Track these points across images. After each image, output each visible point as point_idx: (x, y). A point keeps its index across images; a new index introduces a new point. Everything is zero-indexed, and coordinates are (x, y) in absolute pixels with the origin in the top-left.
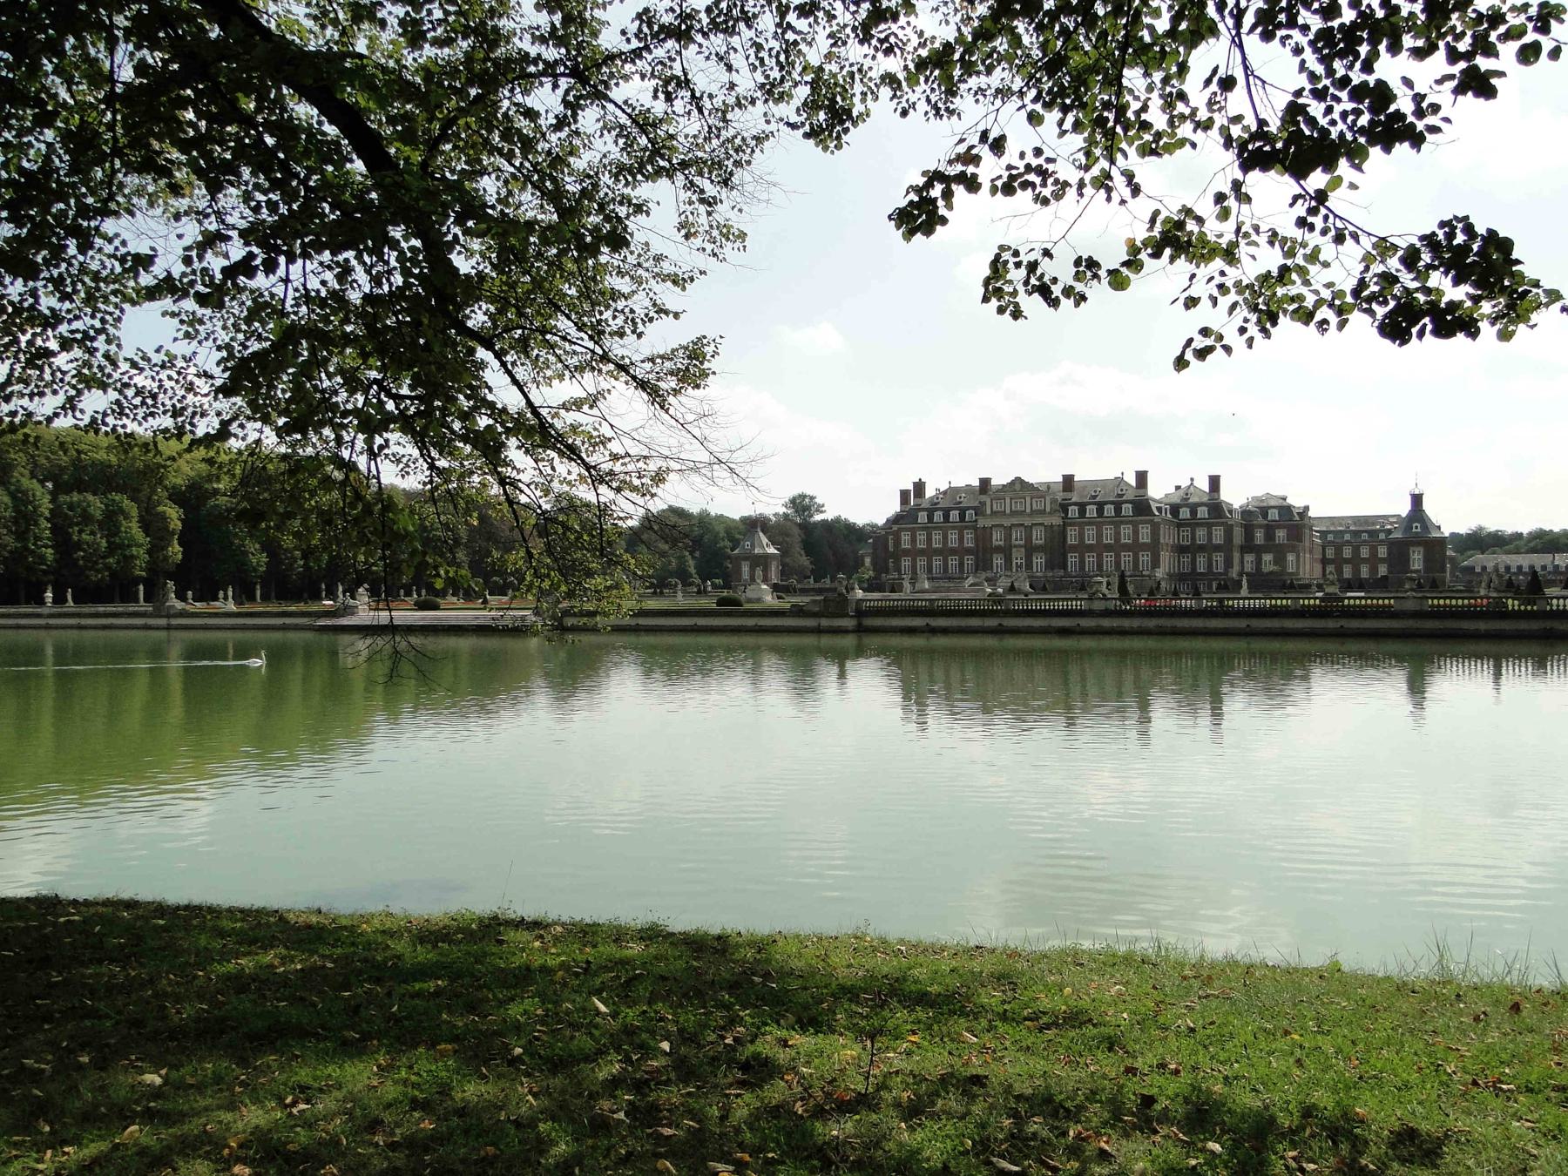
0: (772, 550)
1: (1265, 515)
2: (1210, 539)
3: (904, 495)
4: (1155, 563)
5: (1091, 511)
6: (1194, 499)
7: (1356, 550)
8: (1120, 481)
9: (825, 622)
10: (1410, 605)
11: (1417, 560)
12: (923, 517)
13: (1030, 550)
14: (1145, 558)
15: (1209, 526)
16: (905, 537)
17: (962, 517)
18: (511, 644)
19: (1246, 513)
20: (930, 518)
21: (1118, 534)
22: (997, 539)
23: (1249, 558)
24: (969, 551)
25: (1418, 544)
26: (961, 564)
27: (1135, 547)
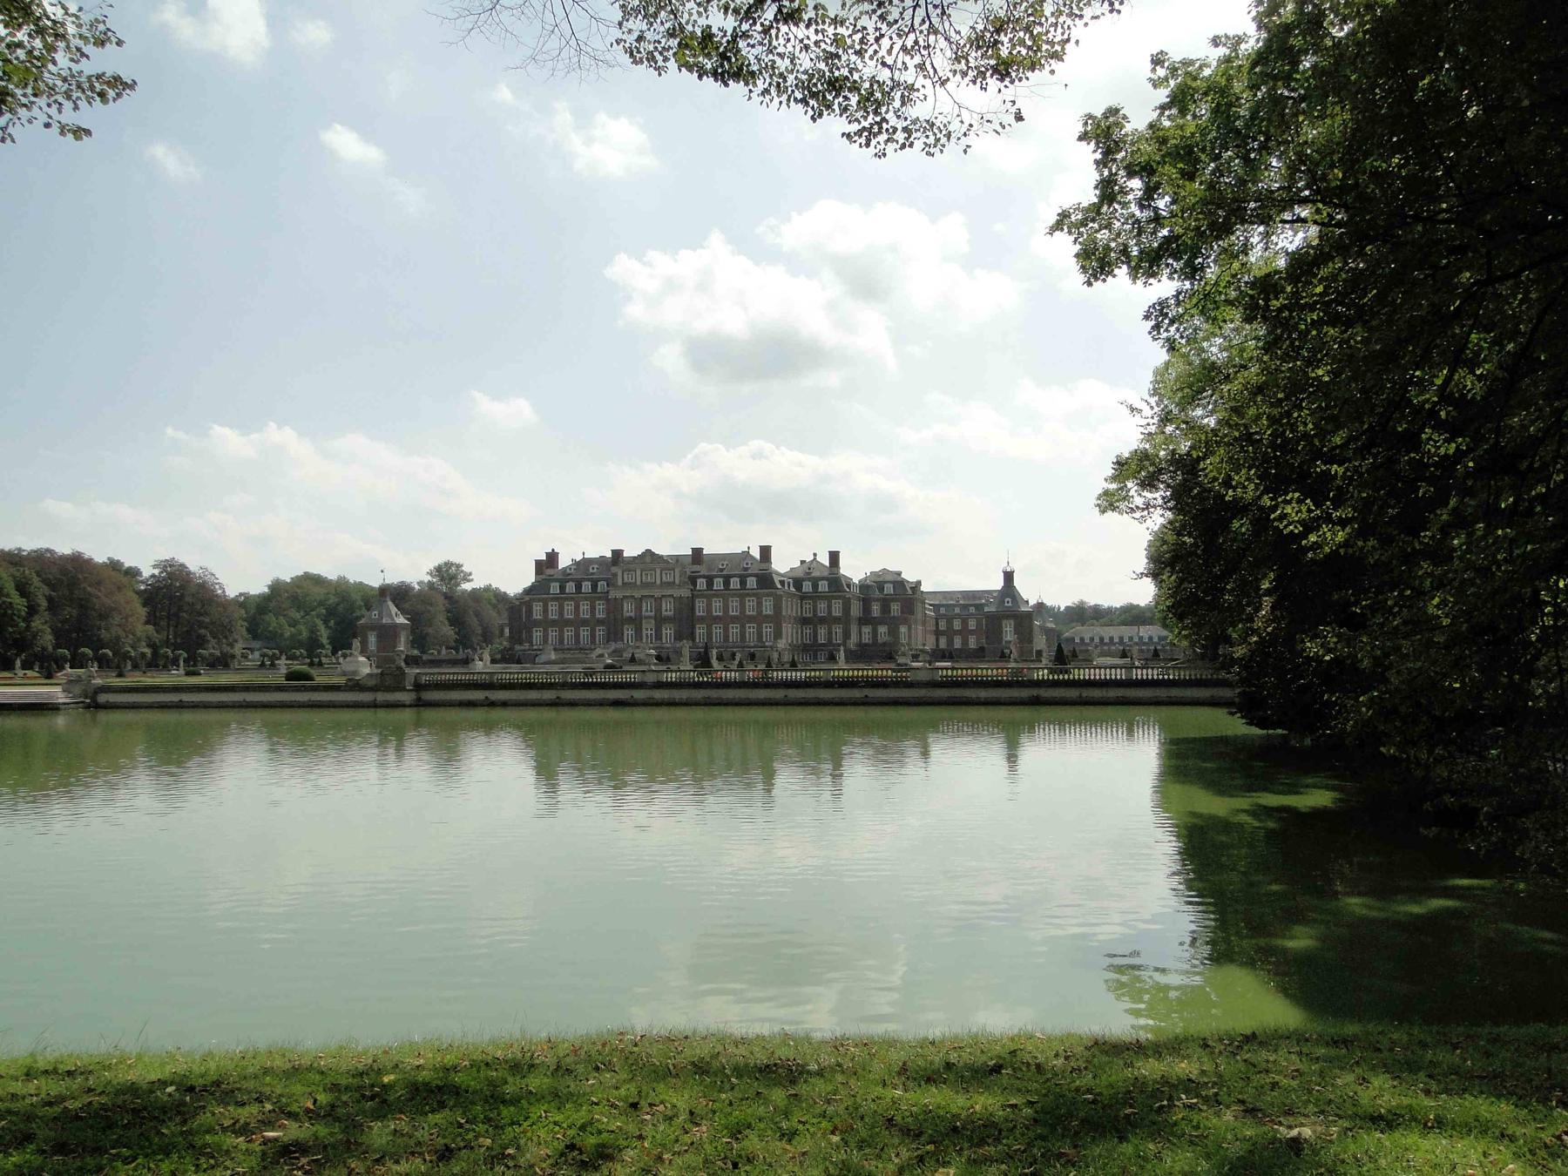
0: (401, 620)
1: (881, 589)
2: (830, 612)
3: (539, 564)
4: (778, 635)
5: (718, 584)
6: (816, 574)
7: (965, 623)
8: (746, 554)
9: (381, 697)
10: (651, 678)
11: (1009, 632)
12: (555, 588)
13: (660, 621)
14: (767, 630)
15: (829, 599)
16: (537, 609)
17: (594, 587)
18: (35, 723)
19: (863, 586)
20: (562, 588)
21: (743, 605)
22: (628, 610)
23: (867, 630)
24: (600, 622)
25: (1008, 617)
26: (593, 636)
27: (759, 619)
